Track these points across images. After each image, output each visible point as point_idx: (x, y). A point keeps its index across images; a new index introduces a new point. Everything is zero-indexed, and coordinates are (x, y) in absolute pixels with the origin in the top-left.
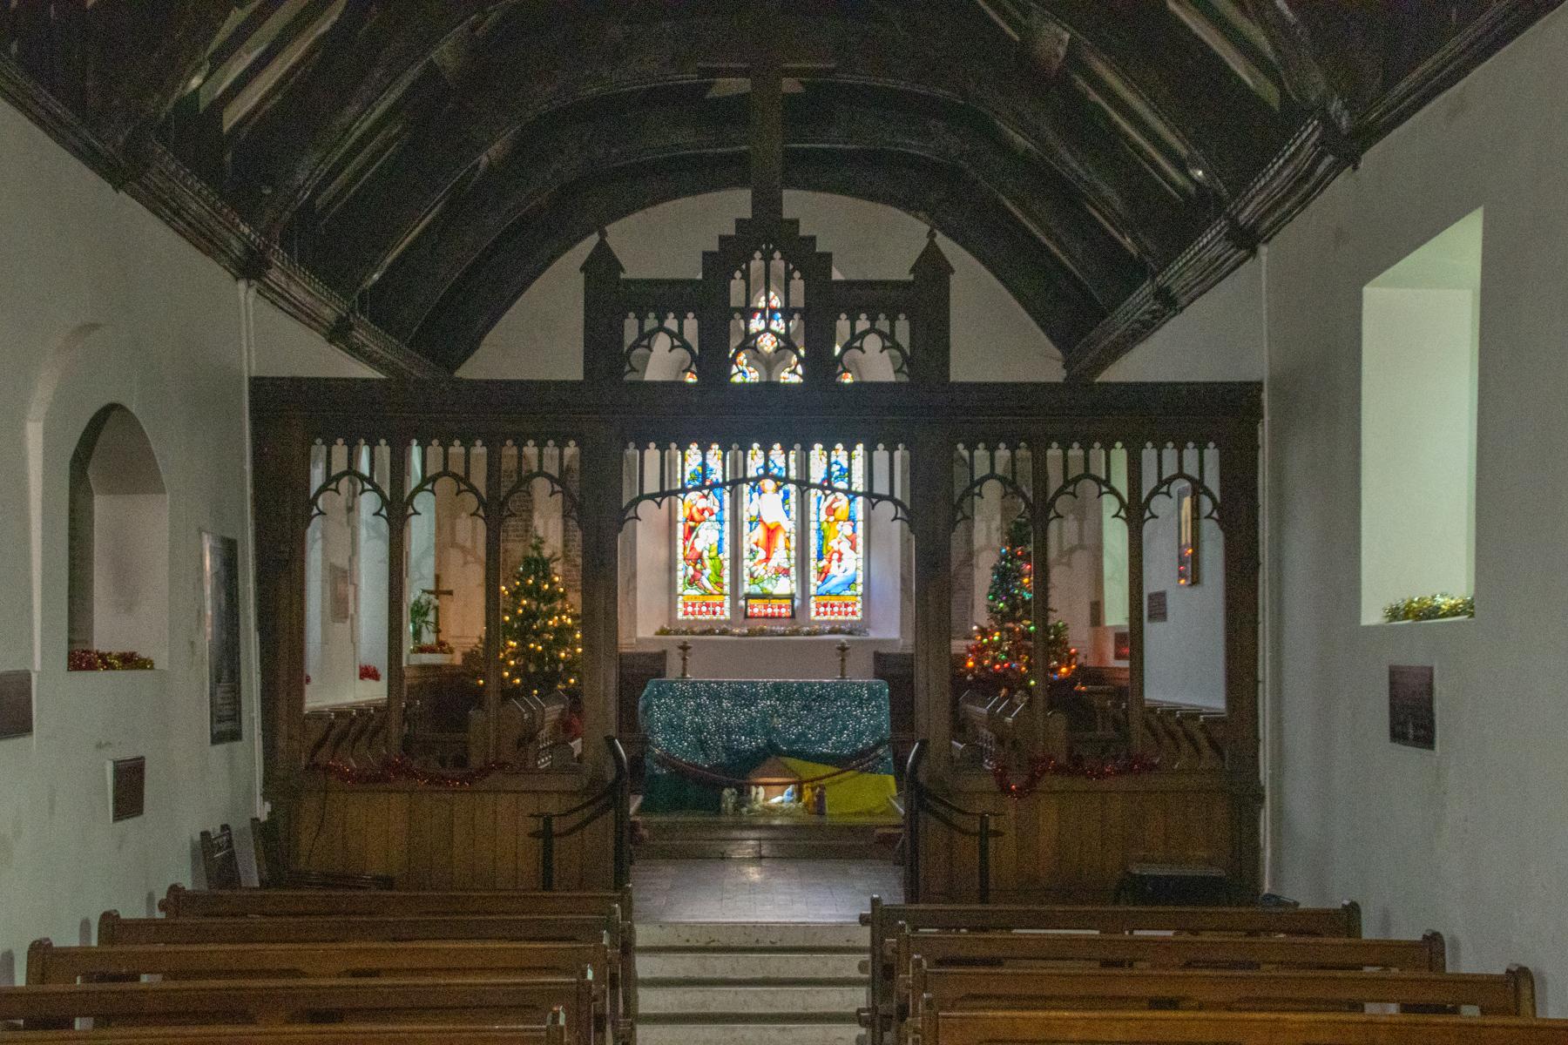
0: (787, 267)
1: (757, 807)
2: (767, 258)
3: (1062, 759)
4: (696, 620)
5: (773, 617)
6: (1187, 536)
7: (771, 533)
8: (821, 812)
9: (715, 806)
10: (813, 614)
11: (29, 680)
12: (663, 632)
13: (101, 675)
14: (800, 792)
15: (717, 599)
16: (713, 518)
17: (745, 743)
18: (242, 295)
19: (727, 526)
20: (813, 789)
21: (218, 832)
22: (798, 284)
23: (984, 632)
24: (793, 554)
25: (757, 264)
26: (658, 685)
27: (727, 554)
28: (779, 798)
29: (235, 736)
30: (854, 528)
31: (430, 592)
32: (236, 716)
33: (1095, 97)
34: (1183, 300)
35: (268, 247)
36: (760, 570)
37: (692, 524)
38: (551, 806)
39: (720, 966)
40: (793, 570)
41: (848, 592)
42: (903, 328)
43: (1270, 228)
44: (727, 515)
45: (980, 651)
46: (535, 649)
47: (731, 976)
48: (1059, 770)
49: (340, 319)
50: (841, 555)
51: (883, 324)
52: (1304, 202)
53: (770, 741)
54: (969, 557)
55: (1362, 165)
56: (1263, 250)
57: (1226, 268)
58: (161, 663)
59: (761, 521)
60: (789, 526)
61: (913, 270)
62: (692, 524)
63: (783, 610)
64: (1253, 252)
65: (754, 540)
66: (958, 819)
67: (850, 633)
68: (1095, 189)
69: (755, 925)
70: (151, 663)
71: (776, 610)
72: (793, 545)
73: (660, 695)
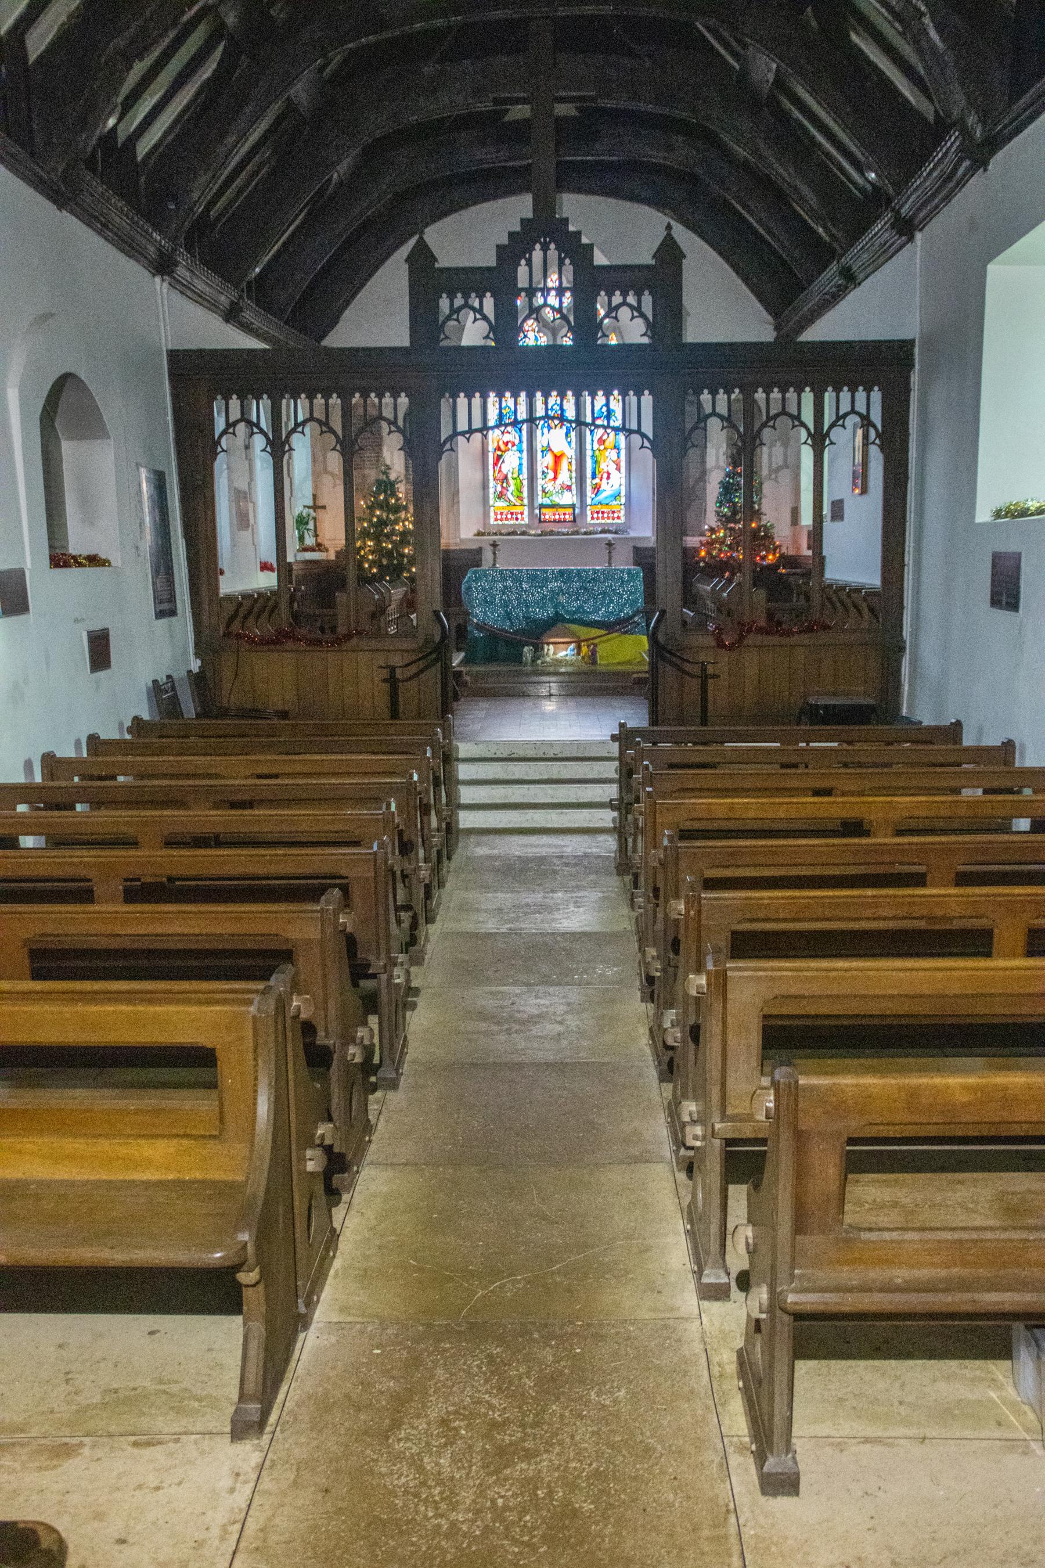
0: (560, 255)
1: (548, 659)
2: (545, 248)
3: (762, 623)
4: (504, 525)
5: (560, 521)
6: (859, 458)
7: (557, 459)
8: (594, 662)
9: (518, 659)
11: (24, 575)
12: (479, 534)
13: (73, 572)
14: (579, 648)
15: (519, 509)
16: (515, 448)
17: (540, 614)
18: (158, 287)
19: (525, 455)
20: (588, 646)
21: (165, 680)
22: (568, 268)
23: (712, 530)
24: (574, 475)
25: (537, 255)
26: (475, 573)
27: (525, 475)
28: (564, 653)
29: (173, 613)
30: (618, 453)
31: (309, 507)
32: (172, 599)
33: (797, 114)
34: (861, 276)
35: (174, 250)
36: (549, 487)
37: (499, 453)
38: (397, 660)
39: (518, 770)
40: (574, 487)
41: (615, 503)
42: (647, 300)
43: (924, 219)
44: (525, 446)
45: (710, 544)
46: (385, 548)
47: (526, 778)
48: (760, 631)
49: (232, 303)
50: (609, 474)
51: (631, 299)
52: (947, 199)
53: (557, 612)
54: (703, 474)
55: (990, 167)
56: (918, 236)
57: (892, 250)
58: (116, 560)
59: (550, 450)
60: (571, 452)
61: (654, 256)
62: (499, 453)
63: (567, 517)
64: (911, 238)
66: (688, 667)
67: (616, 533)
68: (795, 188)
69: (543, 742)
70: (109, 561)
71: (562, 517)
72: (574, 467)
73: (476, 581)
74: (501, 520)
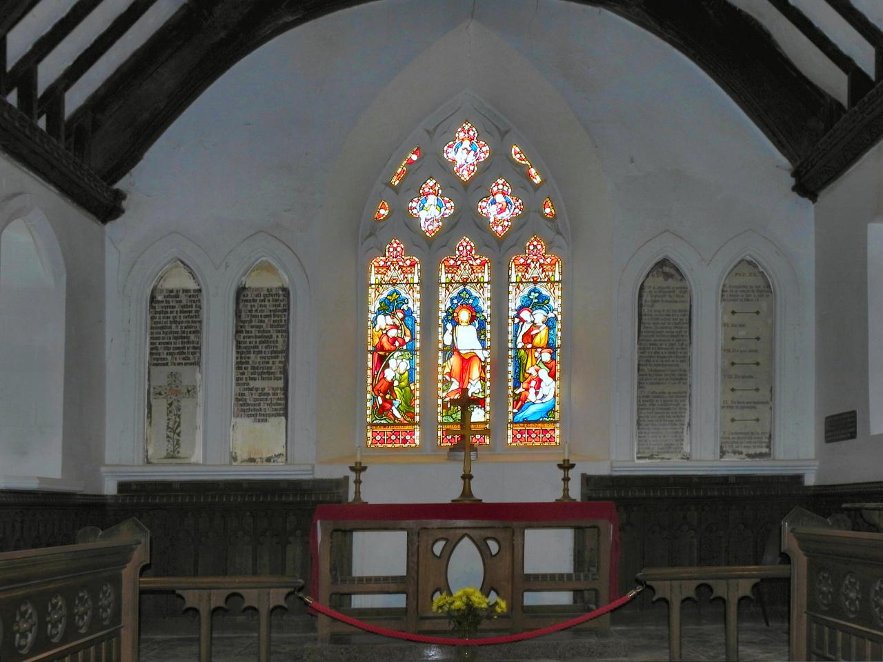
7: (466, 362)
10: (509, 441)
37: (381, 353)
62: (381, 353)
65: (447, 370)
74: (382, 441)
